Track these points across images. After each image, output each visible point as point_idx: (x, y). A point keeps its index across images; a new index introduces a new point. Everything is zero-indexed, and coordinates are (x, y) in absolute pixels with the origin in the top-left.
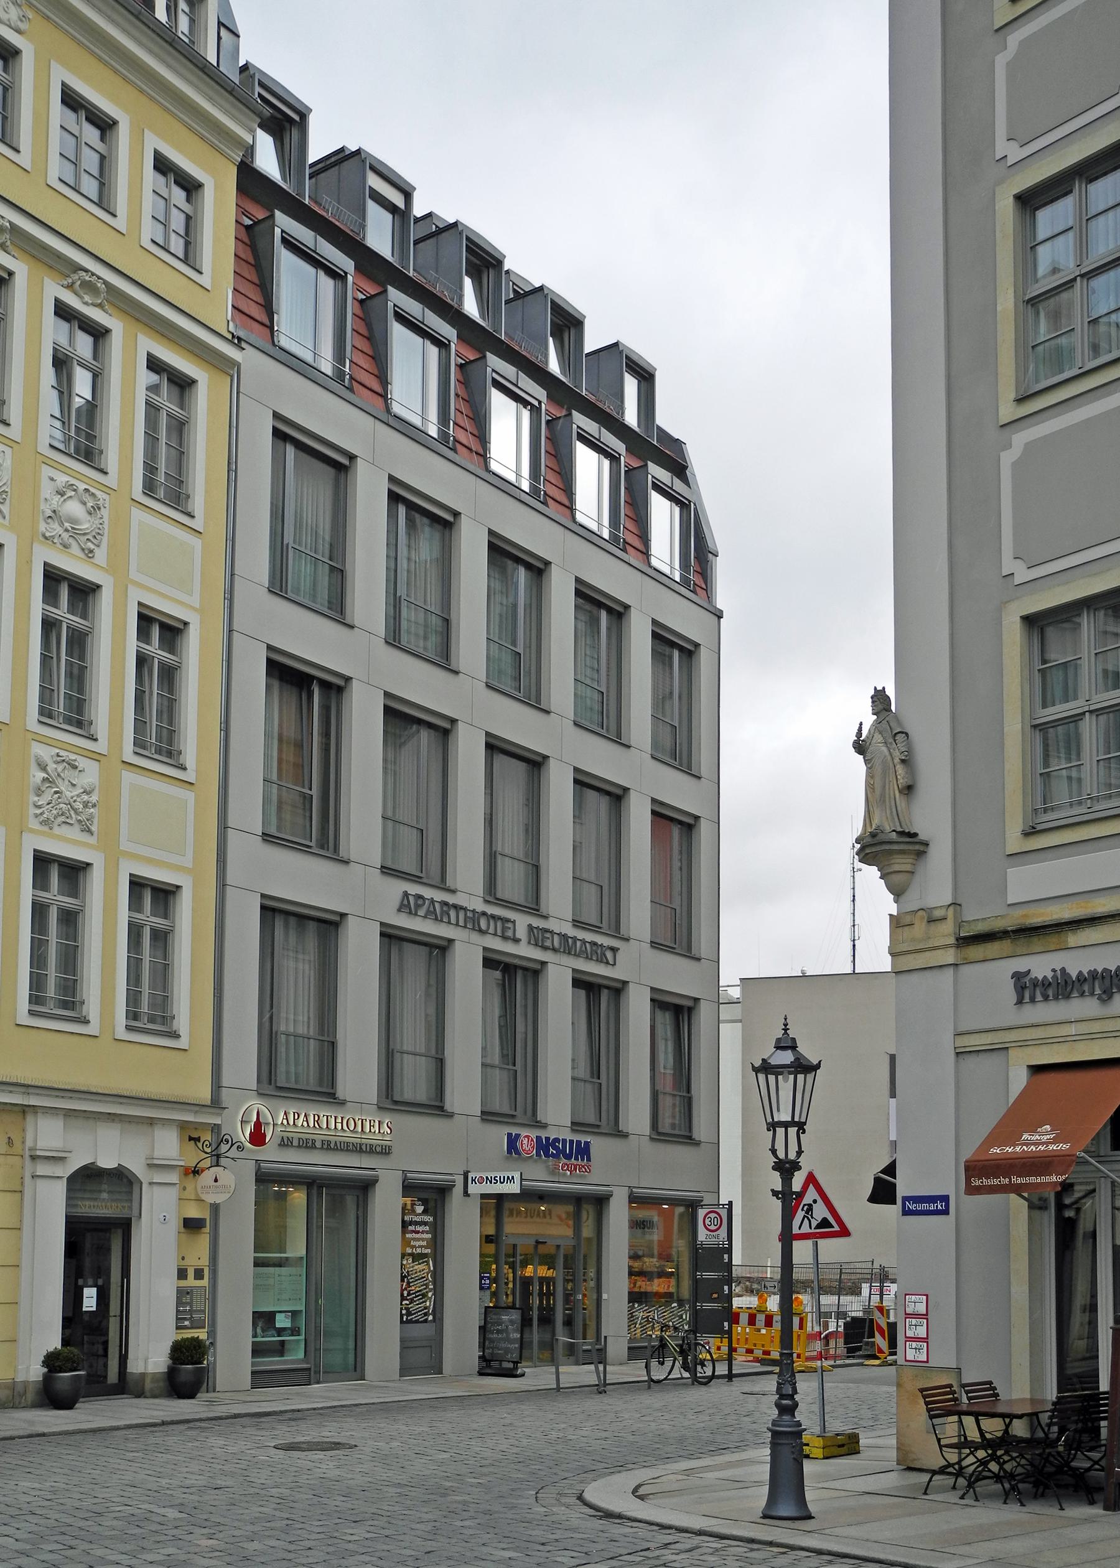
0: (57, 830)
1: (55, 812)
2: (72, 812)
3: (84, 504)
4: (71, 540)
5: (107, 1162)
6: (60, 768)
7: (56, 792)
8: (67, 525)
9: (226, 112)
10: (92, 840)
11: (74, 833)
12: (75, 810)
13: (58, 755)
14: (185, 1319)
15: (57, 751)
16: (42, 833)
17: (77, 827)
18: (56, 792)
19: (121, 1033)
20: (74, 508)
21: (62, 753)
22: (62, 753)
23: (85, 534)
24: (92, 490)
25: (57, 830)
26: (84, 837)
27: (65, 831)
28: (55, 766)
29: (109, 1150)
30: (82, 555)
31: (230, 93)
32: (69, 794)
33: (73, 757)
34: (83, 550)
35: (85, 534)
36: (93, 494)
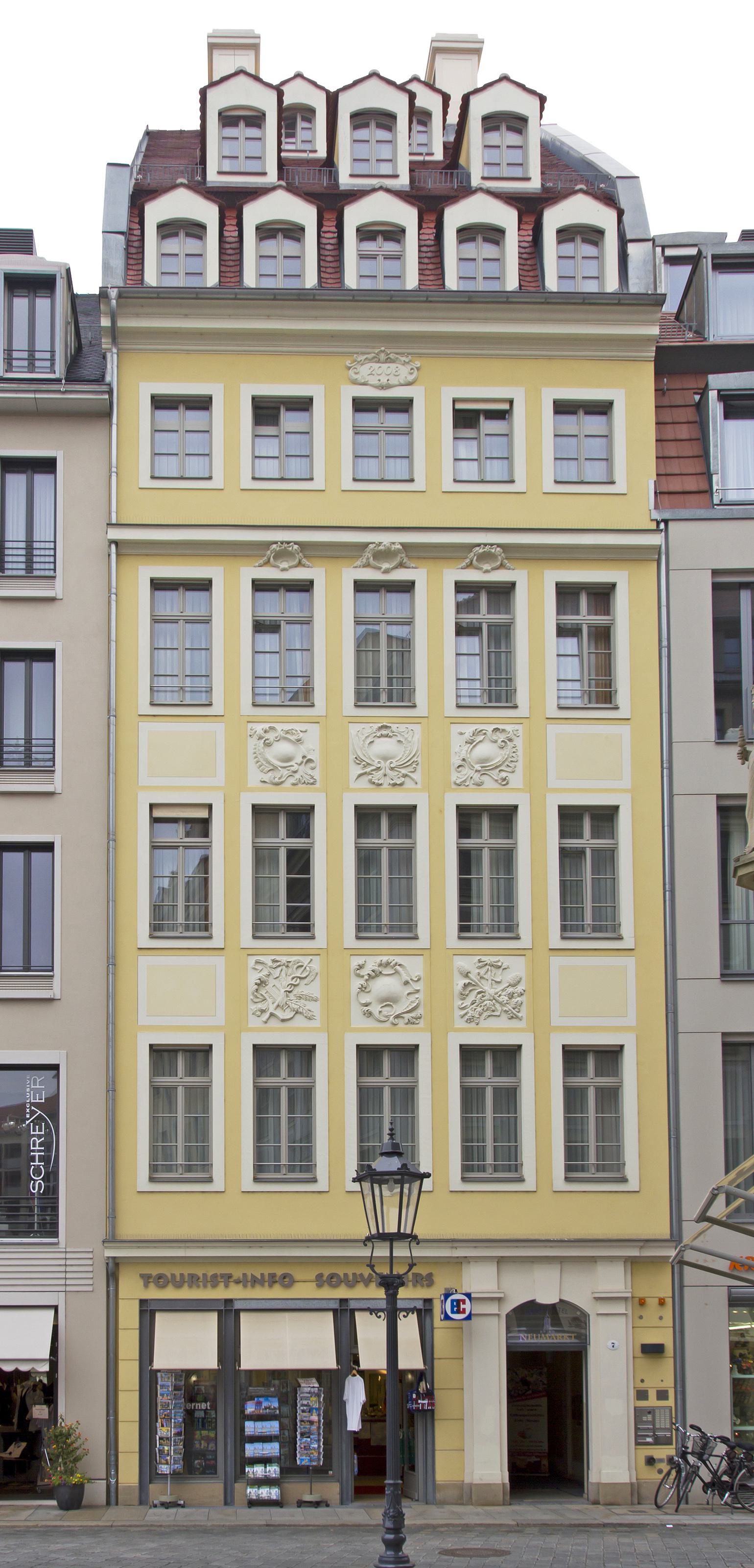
0: (483, 1024)
1: (479, 1009)
2: (498, 1006)
3: (496, 742)
4: (484, 778)
5: (547, 1297)
6: (483, 971)
7: (479, 993)
8: (477, 767)
9: (625, 322)
10: (522, 1024)
11: (503, 1022)
12: (501, 1003)
13: (480, 961)
14: (648, 1436)
15: (479, 957)
16: (469, 1030)
17: (504, 1017)
18: (479, 993)
19: (559, 1183)
20: (485, 749)
21: (483, 958)
22: (483, 958)
23: (497, 767)
24: (501, 727)
25: (483, 1024)
26: (514, 1024)
27: (492, 1023)
28: (478, 971)
29: (544, 1287)
30: (497, 786)
31: (619, 304)
32: (492, 991)
33: (495, 959)
34: (496, 781)
35: (497, 767)
36: (504, 730)
